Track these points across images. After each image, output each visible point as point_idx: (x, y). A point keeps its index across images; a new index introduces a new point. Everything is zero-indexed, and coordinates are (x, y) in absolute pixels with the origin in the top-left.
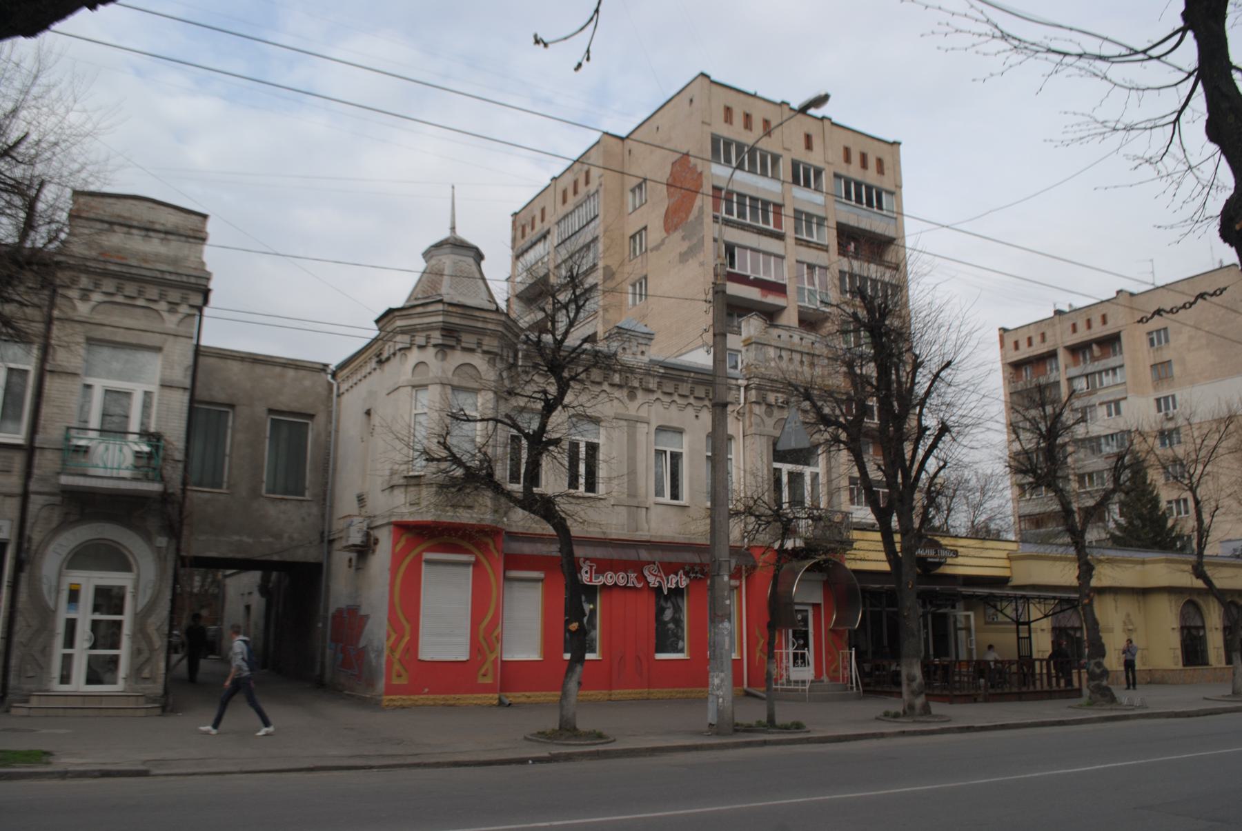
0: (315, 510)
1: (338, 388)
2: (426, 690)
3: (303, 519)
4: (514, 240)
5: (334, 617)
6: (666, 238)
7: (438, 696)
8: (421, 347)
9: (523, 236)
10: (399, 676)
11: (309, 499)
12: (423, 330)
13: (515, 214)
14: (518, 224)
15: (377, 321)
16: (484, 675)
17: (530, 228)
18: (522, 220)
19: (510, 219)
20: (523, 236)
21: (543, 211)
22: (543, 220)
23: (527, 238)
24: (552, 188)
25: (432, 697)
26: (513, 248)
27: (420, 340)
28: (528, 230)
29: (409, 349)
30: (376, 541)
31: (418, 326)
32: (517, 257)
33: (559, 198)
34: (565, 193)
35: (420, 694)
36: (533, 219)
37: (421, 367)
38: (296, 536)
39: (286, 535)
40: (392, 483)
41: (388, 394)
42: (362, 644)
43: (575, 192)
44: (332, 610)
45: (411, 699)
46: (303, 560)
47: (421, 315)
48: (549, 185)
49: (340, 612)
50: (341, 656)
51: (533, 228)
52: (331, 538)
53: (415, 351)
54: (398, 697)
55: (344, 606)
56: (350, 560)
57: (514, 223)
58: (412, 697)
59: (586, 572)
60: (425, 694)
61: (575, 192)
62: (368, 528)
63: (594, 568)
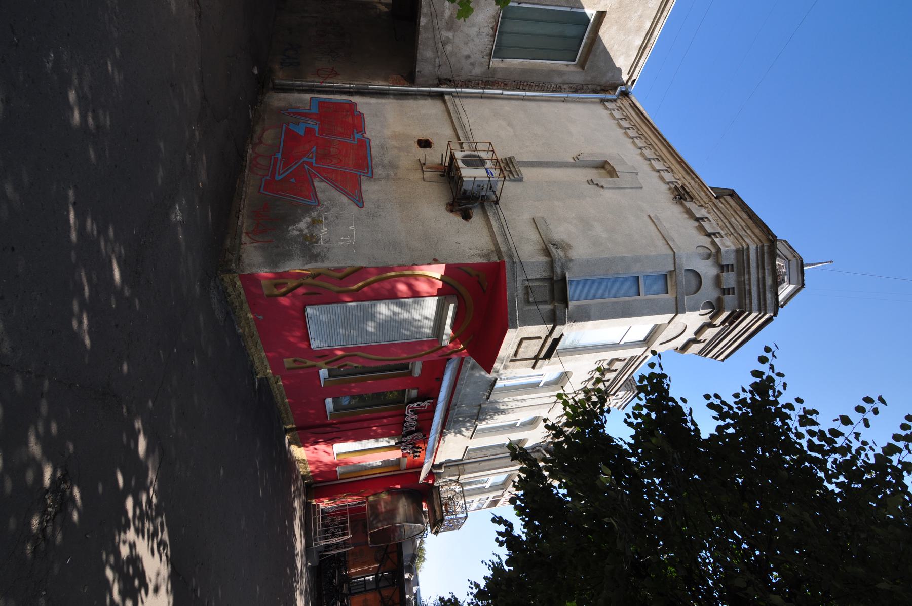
0: (478, 71)
3: (468, 57)
5: (353, 106)
8: (718, 280)
12: (741, 283)
31: (747, 277)
37: (694, 282)
38: (449, 48)
39: (450, 35)
40: (553, 250)
41: (649, 216)
45: (242, 303)
46: (419, 57)
47: (761, 281)
52: (447, 97)
55: (368, 135)
59: (419, 405)
62: (482, 196)
63: (423, 409)
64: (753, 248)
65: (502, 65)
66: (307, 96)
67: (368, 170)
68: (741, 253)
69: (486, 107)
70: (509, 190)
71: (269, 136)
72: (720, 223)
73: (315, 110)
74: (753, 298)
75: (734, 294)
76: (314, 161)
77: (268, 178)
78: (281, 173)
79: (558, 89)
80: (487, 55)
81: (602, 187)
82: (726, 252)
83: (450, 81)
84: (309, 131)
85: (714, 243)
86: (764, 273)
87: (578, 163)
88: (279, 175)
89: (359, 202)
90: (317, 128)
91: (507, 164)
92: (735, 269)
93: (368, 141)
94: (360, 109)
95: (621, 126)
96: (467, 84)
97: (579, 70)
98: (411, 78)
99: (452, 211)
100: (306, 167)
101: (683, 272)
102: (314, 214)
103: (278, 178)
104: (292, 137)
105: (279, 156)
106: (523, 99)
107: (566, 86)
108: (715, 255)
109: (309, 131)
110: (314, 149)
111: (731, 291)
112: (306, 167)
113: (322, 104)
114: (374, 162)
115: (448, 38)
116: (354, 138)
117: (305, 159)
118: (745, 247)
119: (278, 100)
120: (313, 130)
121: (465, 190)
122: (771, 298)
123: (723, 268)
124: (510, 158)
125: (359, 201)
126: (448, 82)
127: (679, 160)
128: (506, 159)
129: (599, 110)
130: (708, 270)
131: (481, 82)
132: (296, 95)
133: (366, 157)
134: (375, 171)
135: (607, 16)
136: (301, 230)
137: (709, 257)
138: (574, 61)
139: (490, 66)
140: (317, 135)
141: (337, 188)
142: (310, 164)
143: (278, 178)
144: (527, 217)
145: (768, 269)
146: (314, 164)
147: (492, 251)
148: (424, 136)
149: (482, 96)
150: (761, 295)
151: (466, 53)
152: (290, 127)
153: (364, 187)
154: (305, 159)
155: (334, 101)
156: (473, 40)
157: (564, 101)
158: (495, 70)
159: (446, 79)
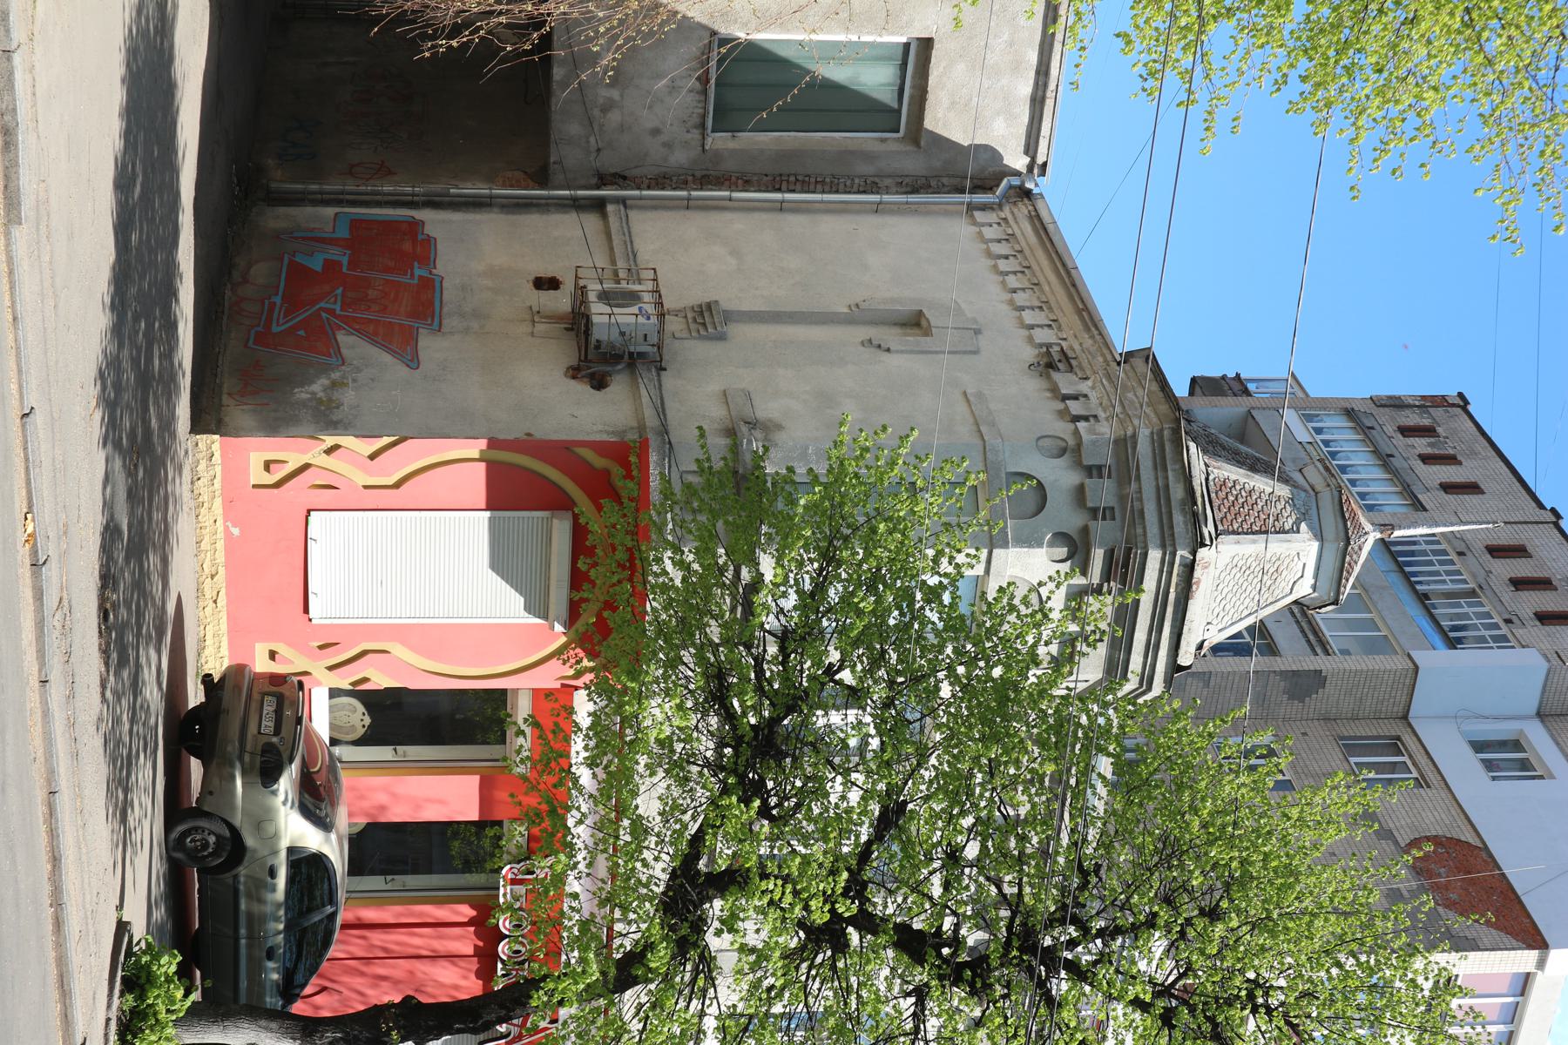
0: (680, 158)
1: (984, 207)
2: (236, 531)
3: (656, 132)
4: (1396, 404)
5: (415, 226)
6: (1396, 843)
7: (221, 557)
9: (1406, 431)
10: (267, 466)
11: (709, 141)
13: (1463, 402)
14: (1438, 413)
15: (1147, 355)
16: (273, 655)
17: (1429, 450)
18: (1452, 428)
19: (1451, 392)
20: (1406, 431)
21: (1472, 488)
22: (1448, 488)
23: (1399, 440)
24: (1532, 512)
25: (220, 545)
26: (1377, 402)
27: (1104, 492)
28: (1421, 445)
29: (1078, 463)
30: (599, 383)
32: (1350, 413)
33: (1506, 537)
34: (1519, 551)
35: (226, 519)
36: (1451, 460)
38: (614, 117)
39: (615, 94)
41: (965, 393)
42: (349, 343)
43: (1519, 584)
44: (434, 221)
47: (1163, 494)
48: (1541, 506)
49: (424, 250)
50: (316, 264)
51: (1426, 459)
53: (1071, 478)
54: (218, 469)
55: (441, 268)
56: (552, 284)
57: (1440, 402)
58: (218, 502)
60: (226, 529)
61: (1519, 584)
64: (1144, 435)
65: (732, 145)
66: (330, 211)
67: (433, 321)
68: (1124, 445)
69: (691, 226)
70: (690, 351)
71: (260, 272)
72: (1105, 402)
73: (343, 232)
74: (1148, 524)
75: (1113, 519)
76: (337, 307)
77: (259, 329)
78: (281, 321)
79: (871, 187)
80: (696, 127)
81: (888, 350)
82: (1094, 443)
83: (625, 178)
84: (331, 266)
85: (1076, 432)
86: (1167, 478)
87: (857, 316)
88: (278, 325)
89: (413, 362)
90: (345, 261)
91: (701, 313)
92: (1114, 474)
93: (438, 280)
94: (429, 230)
95: (989, 254)
96: (660, 181)
97: (910, 148)
98: (542, 177)
99: (574, 377)
100: (324, 315)
101: (1004, 476)
102: (336, 375)
103: (275, 329)
104: (299, 274)
105: (278, 300)
106: (781, 207)
107: (888, 182)
108: (1072, 451)
109: (331, 266)
110: (339, 291)
111: (1107, 512)
112: (324, 315)
113: (356, 224)
114: (445, 310)
115: (611, 100)
116: (412, 275)
117: (322, 305)
118: (1129, 432)
119: (277, 218)
120: (340, 264)
121: (598, 341)
122: (1185, 523)
123: (1094, 471)
124: (709, 305)
125: (412, 361)
126: (621, 181)
127: (1081, 306)
128: (700, 306)
129: (962, 229)
130: (1059, 476)
131: (690, 178)
132: (306, 212)
133: (431, 303)
134: (445, 322)
135: (936, 46)
136: (313, 393)
137: (1062, 452)
138: (898, 131)
139: (707, 147)
140: (344, 269)
141: (375, 343)
142: (332, 312)
143: (275, 329)
144: (715, 387)
145: (1173, 470)
146: (338, 312)
147: (632, 428)
148: (546, 271)
149: (688, 205)
150: (1164, 517)
151: (650, 125)
152: (297, 259)
153: (420, 344)
154: (322, 305)
155: (380, 218)
156: (662, 101)
157: (877, 209)
158: (717, 156)
159: (615, 175)
